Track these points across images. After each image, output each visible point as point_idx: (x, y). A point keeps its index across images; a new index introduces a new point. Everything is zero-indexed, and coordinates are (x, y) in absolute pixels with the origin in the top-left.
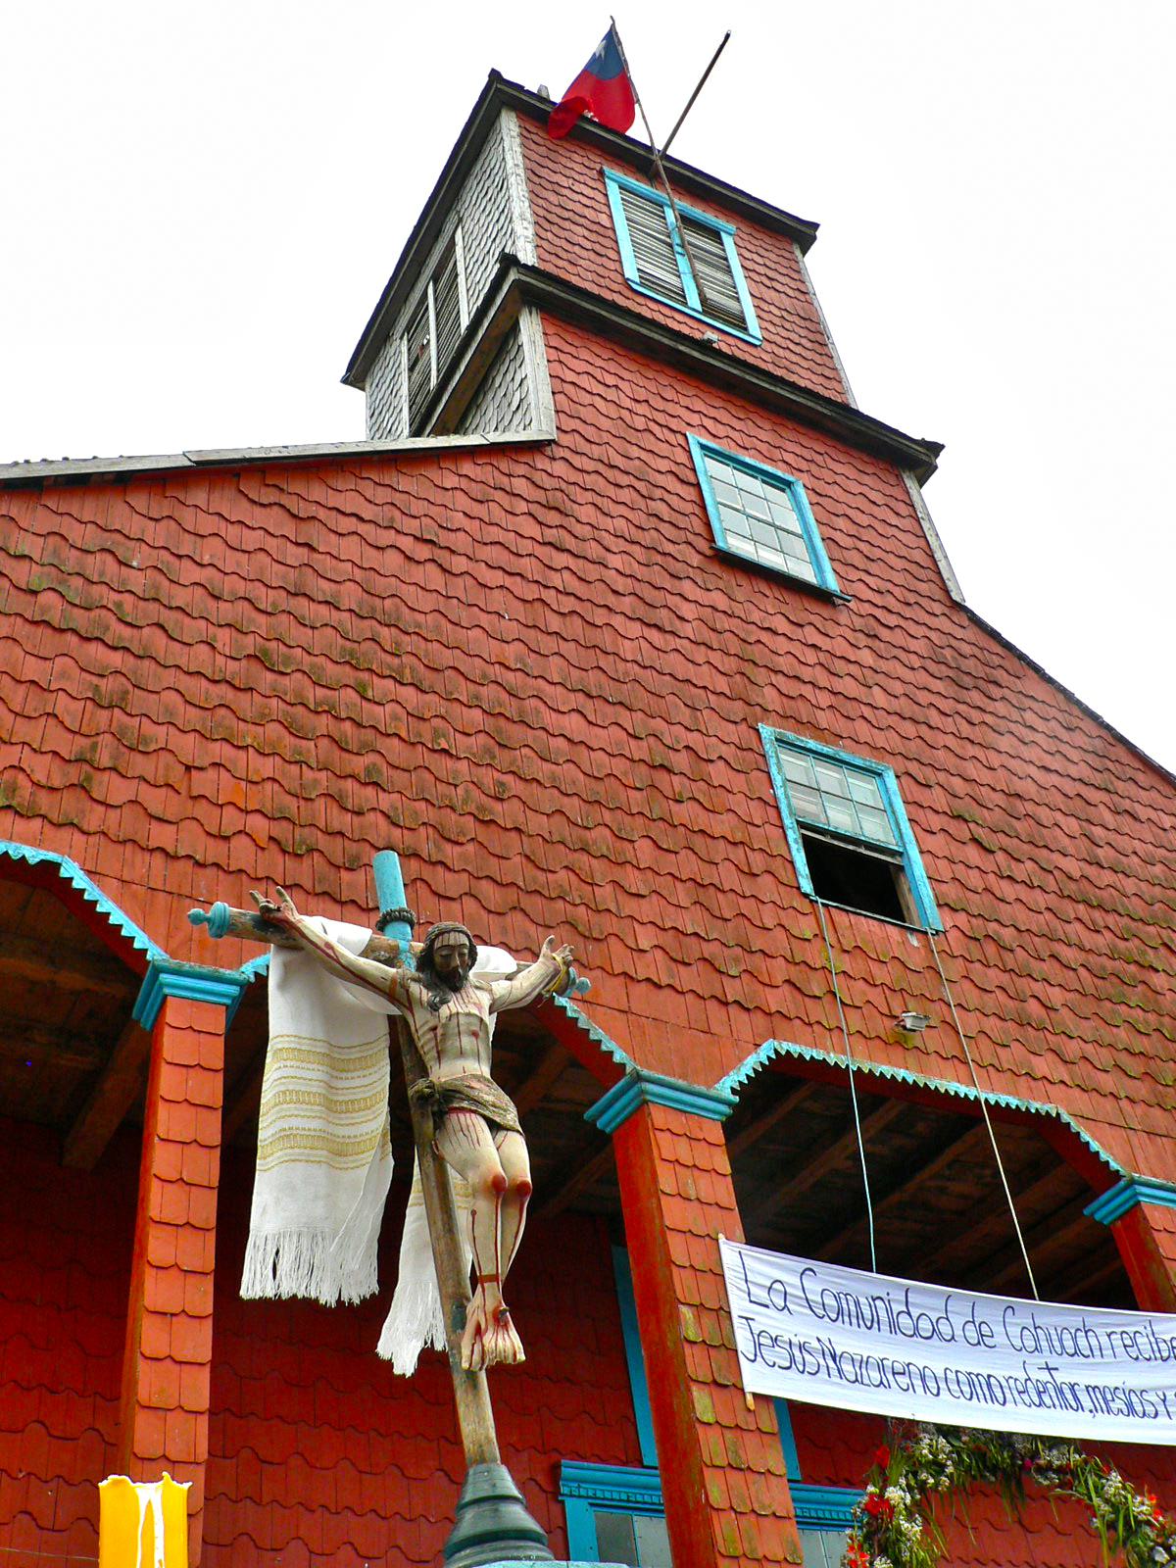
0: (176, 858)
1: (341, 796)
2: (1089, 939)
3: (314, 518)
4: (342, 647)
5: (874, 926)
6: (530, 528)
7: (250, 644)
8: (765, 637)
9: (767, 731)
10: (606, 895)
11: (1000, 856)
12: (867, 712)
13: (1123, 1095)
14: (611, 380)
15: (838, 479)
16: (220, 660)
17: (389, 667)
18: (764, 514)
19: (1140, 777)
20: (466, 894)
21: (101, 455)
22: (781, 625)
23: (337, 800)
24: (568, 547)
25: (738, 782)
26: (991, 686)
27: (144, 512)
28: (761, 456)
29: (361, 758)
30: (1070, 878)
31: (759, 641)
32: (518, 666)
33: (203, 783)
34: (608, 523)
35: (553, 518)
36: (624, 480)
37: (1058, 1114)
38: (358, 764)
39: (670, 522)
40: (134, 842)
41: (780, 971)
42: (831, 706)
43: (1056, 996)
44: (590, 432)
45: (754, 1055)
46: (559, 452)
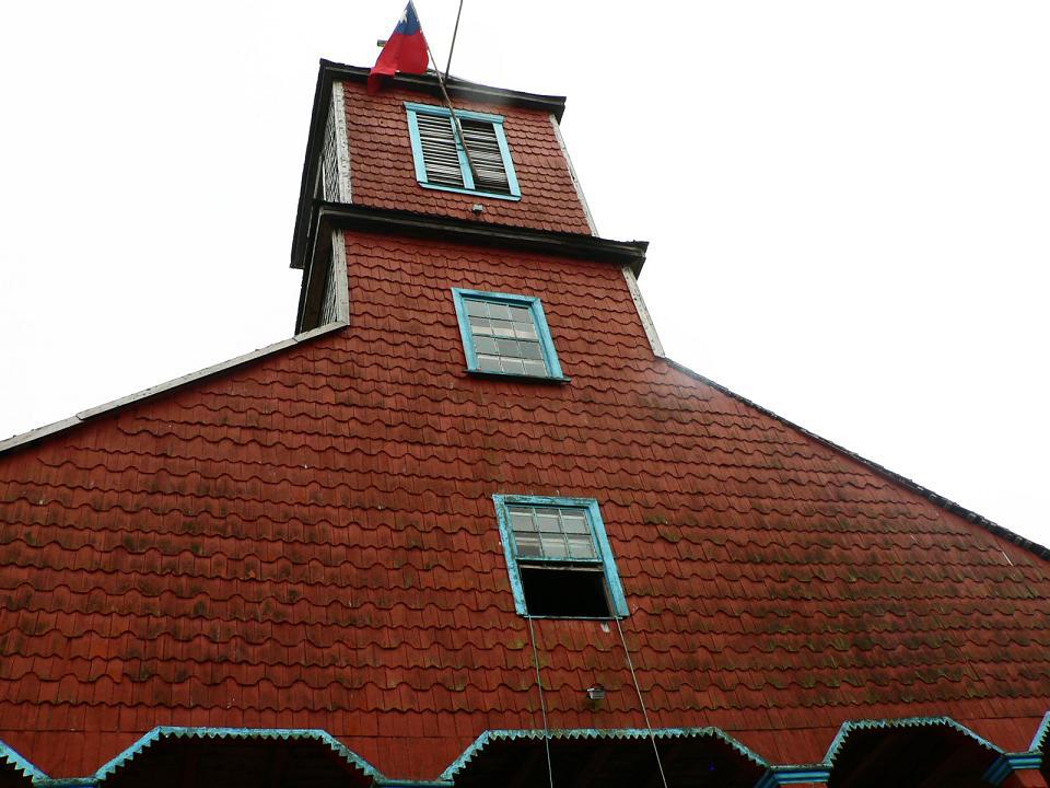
0: (56, 705)
1: (175, 633)
2: (750, 588)
3: (170, 433)
4: (184, 523)
5: (574, 625)
6: (329, 396)
7: (117, 538)
8: (503, 427)
9: (498, 499)
10: (366, 655)
11: (682, 545)
12: (580, 462)
13: (771, 705)
14: (395, 266)
15: (570, 288)
16: (97, 555)
17: (216, 528)
18: (503, 330)
19: (806, 451)
20: (262, 679)
21: (17, 434)
22: (517, 414)
23: (173, 635)
24: (355, 402)
25: (475, 543)
26: (683, 414)
27: (50, 463)
28: (509, 289)
29: (191, 601)
30: (740, 546)
31: (498, 432)
32: (312, 501)
33: (78, 647)
34: (387, 375)
35: (345, 383)
36: (400, 339)
37: (715, 734)
38: (189, 606)
39: (435, 361)
40: (28, 701)
41: (495, 678)
42: (553, 465)
43: (719, 641)
44: (375, 310)
45: (473, 746)
46: (355, 332)
